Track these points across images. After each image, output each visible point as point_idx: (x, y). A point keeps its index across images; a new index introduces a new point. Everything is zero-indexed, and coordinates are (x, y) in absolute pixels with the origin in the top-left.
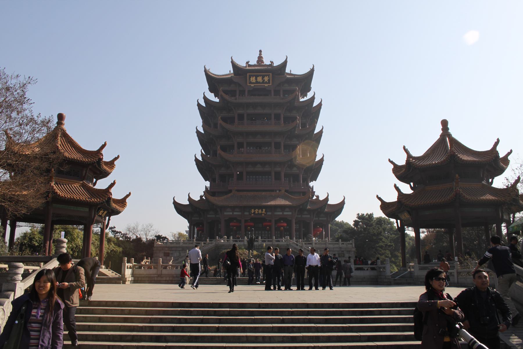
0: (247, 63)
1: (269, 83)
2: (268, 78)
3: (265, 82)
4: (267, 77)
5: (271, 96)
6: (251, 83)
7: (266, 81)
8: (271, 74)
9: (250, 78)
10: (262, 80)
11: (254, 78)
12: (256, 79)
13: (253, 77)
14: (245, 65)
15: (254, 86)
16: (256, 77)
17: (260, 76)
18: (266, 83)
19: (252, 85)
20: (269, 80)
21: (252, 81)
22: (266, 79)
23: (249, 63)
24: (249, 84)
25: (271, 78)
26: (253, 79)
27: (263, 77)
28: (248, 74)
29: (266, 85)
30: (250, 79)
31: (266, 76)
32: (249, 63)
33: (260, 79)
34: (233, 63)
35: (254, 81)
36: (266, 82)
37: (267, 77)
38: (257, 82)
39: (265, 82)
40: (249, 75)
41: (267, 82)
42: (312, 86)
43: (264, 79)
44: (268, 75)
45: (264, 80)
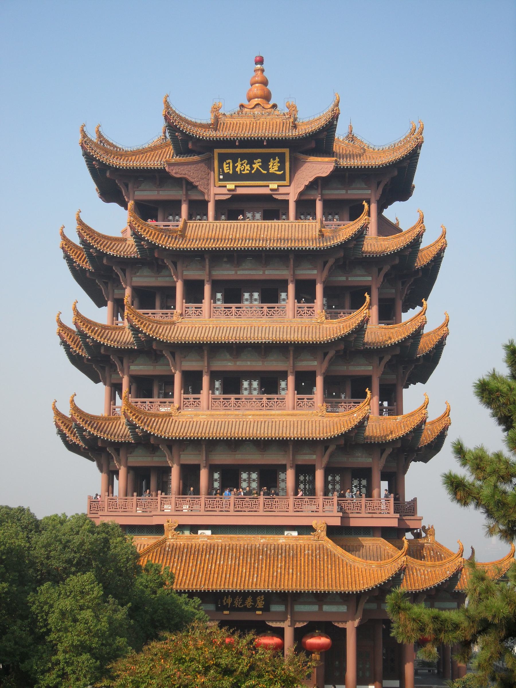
0: (216, 109)
1: (282, 178)
4: (277, 159)
5: (288, 219)
8: (287, 151)
14: (207, 118)
15: (236, 186)
19: (231, 186)
20: (282, 168)
23: (221, 111)
27: (266, 160)
28: (217, 151)
29: (274, 185)
30: (221, 166)
31: (273, 156)
32: (221, 111)
40: (220, 154)
42: (414, 183)
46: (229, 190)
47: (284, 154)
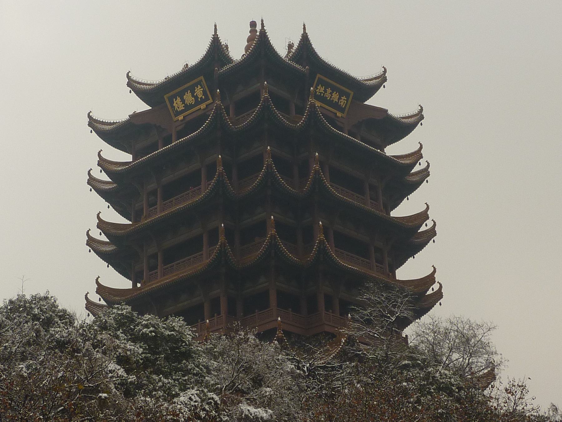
1: (207, 99)
2: (202, 89)
3: (199, 99)
4: (199, 87)
6: (178, 113)
7: (200, 97)
8: (202, 78)
9: (172, 103)
10: (193, 98)
11: (179, 99)
12: (183, 101)
13: (176, 101)
16: (181, 95)
17: (185, 90)
18: (203, 101)
19: (181, 118)
21: (179, 108)
22: (199, 92)
24: (176, 116)
25: (207, 89)
26: (178, 104)
28: (165, 97)
31: (196, 85)
33: (189, 98)
34: (132, 84)
35: (182, 108)
36: (201, 98)
37: (199, 87)
38: (188, 107)
39: (199, 99)
40: (169, 98)
41: (203, 97)
43: (195, 94)
44: (199, 83)
45: (196, 97)
46: (182, 121)
47: (201, 81)
